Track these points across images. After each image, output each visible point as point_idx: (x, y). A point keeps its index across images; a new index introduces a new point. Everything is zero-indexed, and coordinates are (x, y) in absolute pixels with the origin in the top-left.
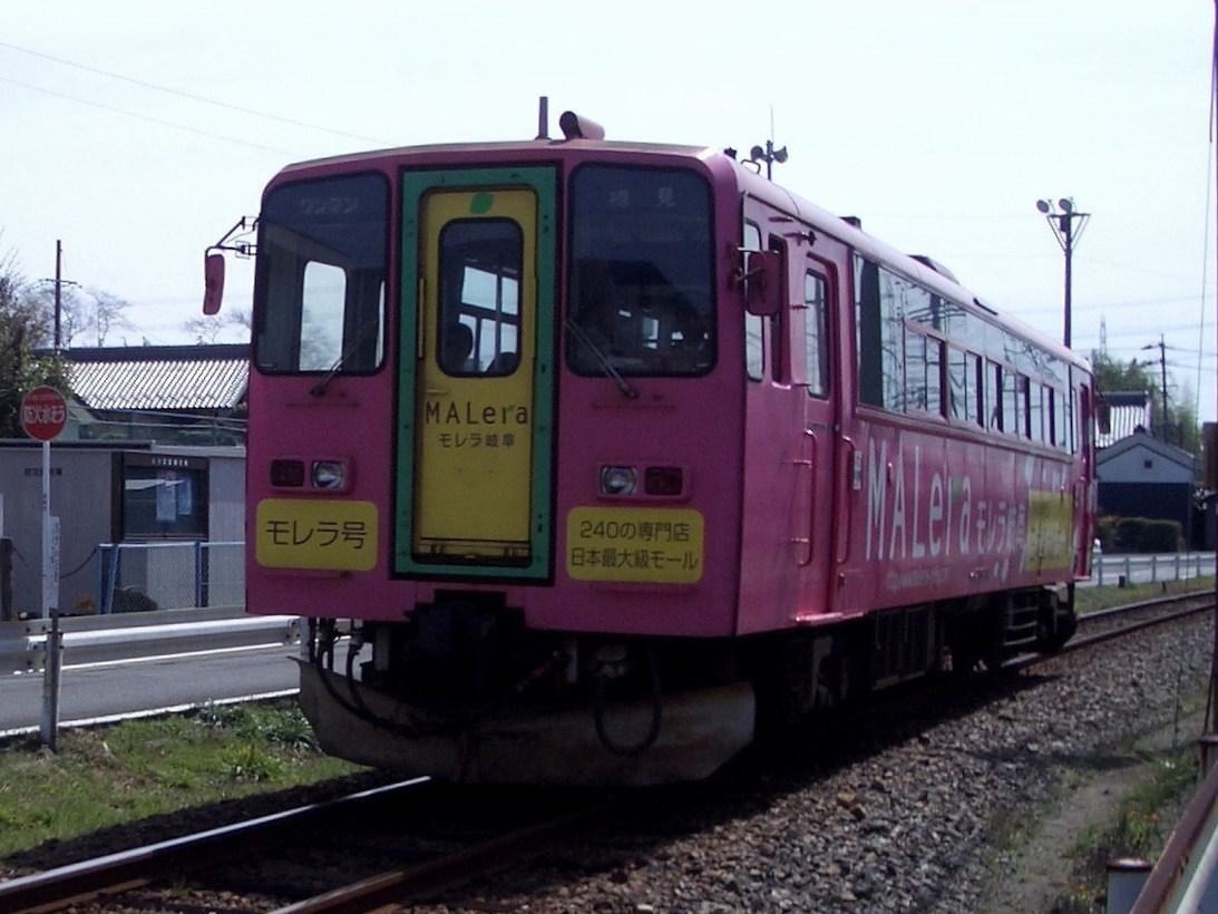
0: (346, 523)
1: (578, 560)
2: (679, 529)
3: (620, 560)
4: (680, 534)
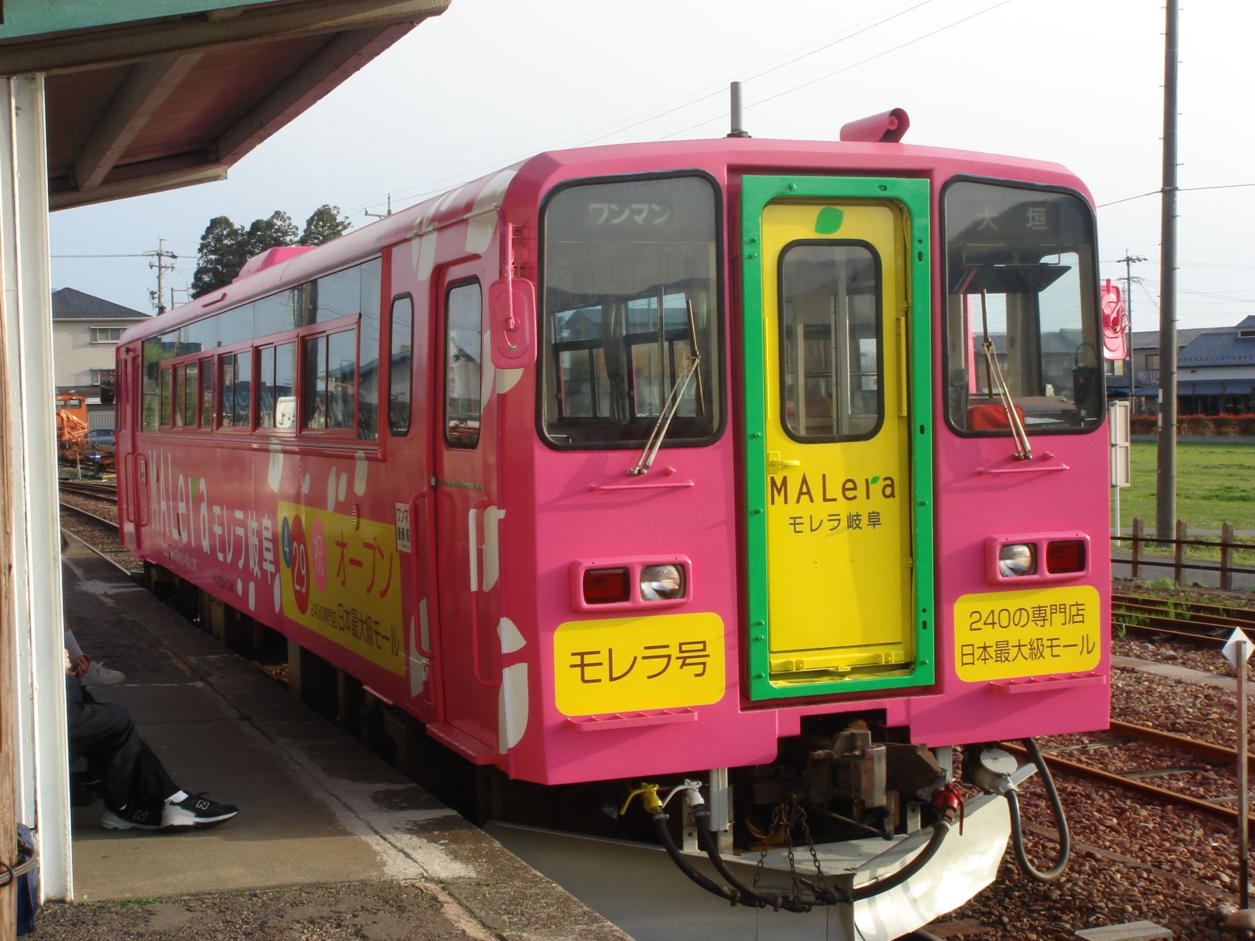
0: (681, 644)
1: (968, 659)
2: (1074, 611)
3: (1014, 651)
4: (1075, 614)
